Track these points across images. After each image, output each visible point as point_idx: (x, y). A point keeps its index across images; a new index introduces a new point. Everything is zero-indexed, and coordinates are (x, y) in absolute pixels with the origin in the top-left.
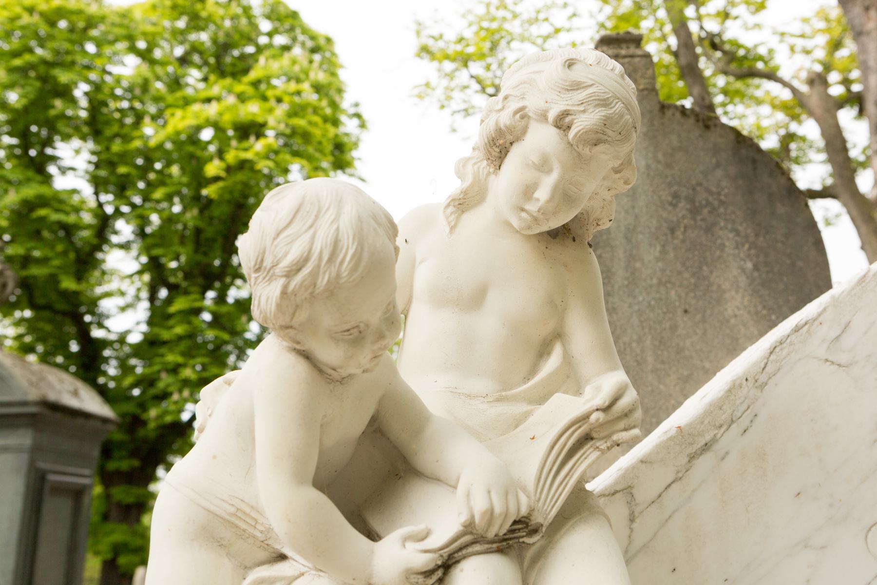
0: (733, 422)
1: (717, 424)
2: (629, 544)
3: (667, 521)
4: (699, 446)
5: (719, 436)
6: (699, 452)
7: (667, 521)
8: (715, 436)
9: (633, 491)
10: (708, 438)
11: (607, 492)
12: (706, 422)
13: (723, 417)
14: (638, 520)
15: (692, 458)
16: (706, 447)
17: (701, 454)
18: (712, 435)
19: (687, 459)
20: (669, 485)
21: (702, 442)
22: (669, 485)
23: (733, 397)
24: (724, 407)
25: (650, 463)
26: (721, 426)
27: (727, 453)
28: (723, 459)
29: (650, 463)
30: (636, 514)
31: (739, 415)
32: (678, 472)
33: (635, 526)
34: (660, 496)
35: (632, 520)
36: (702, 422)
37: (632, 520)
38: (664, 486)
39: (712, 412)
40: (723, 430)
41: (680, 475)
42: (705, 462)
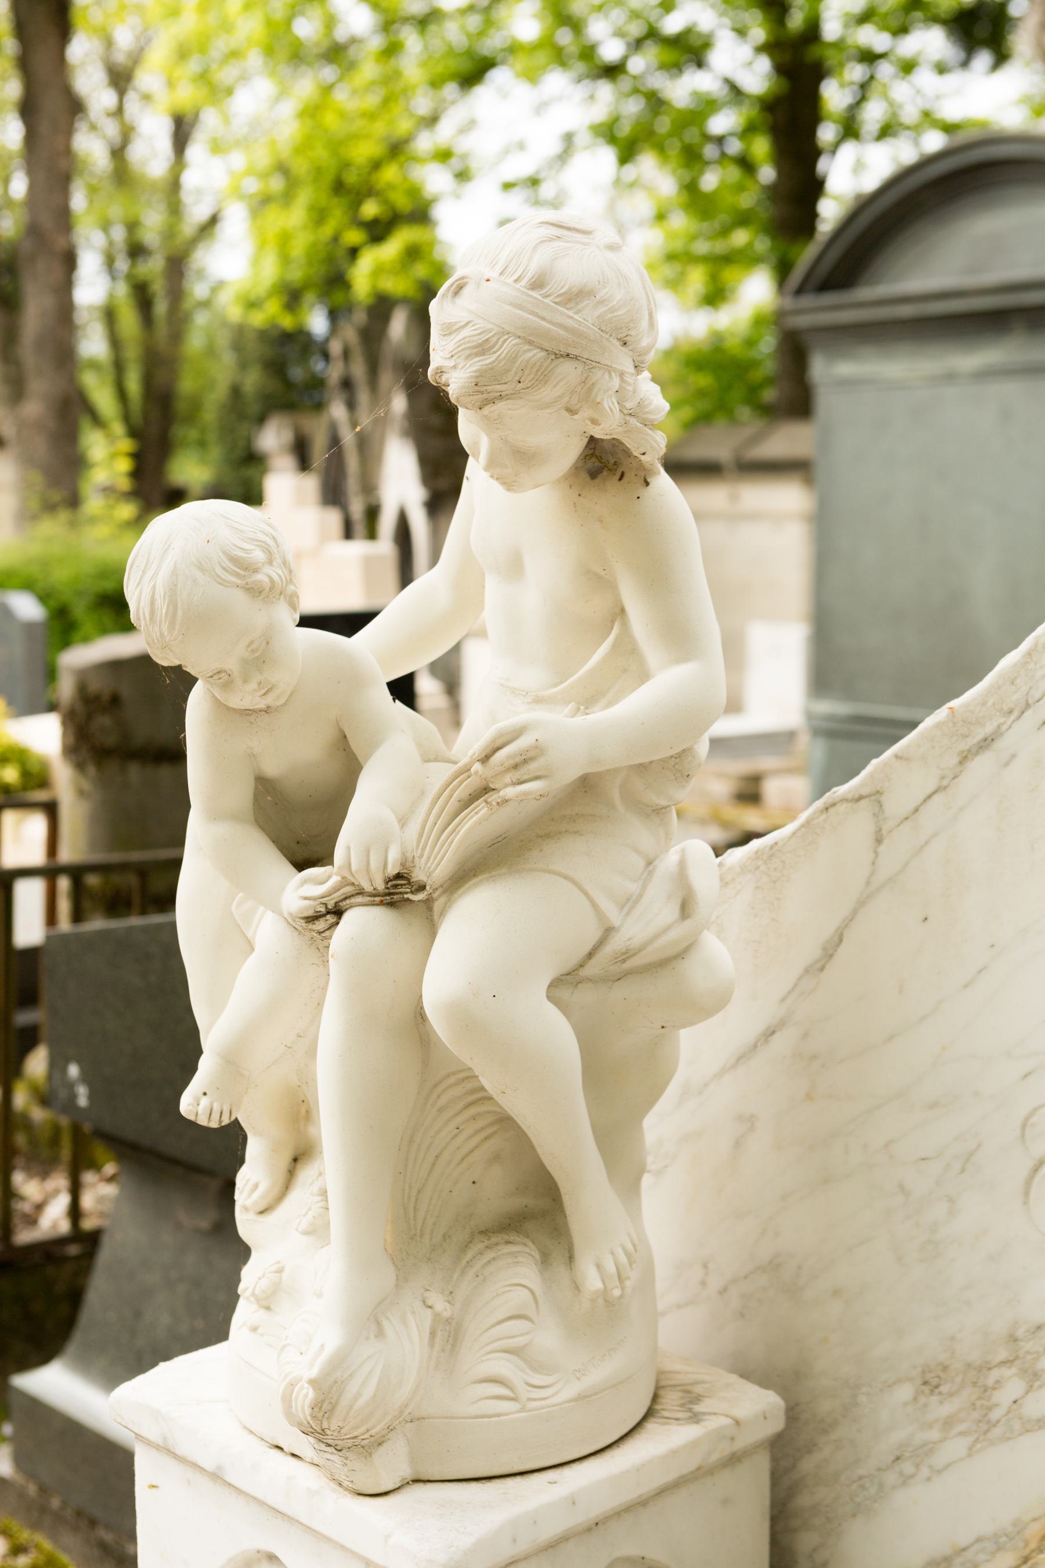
0: (1028, 706)
1: (1005, 708)
2: (872, 873)
3: (922, 848)
4: (975, 741)
5: (1004, 728)
6: (974, 750)
7: (922, 848)
8: (999, 727)
9: (883, 799)
10: (989, 728)
11: (850, 796)
12: (990, 703)
13: (1015, 697)
14: (885, 842)
15: (965, 758)
16: (986, 743)
17: (977, 753)
18: (996, 724)
19: (956, 760)
20: (930, 796)
21: (979, 734)
22: (930, 796)
23: (1032, 666)
24: (1018, 681)
25: (907, 759)
26: (1010, 712)
27: (1014, 756)
28: (1007, 764)
29: (907, 759)
30: (884, 832)
31: (1038, 695)
32: (943, 778)
33: (882, 849)
34: (916, 810)
35: (879, 841)
36: (984, 704)
37: (879, 841)
38: (922, 797)
39: (999, 688)
40: (1013, 717)
41: (945, 783)
42: (982, 765)
